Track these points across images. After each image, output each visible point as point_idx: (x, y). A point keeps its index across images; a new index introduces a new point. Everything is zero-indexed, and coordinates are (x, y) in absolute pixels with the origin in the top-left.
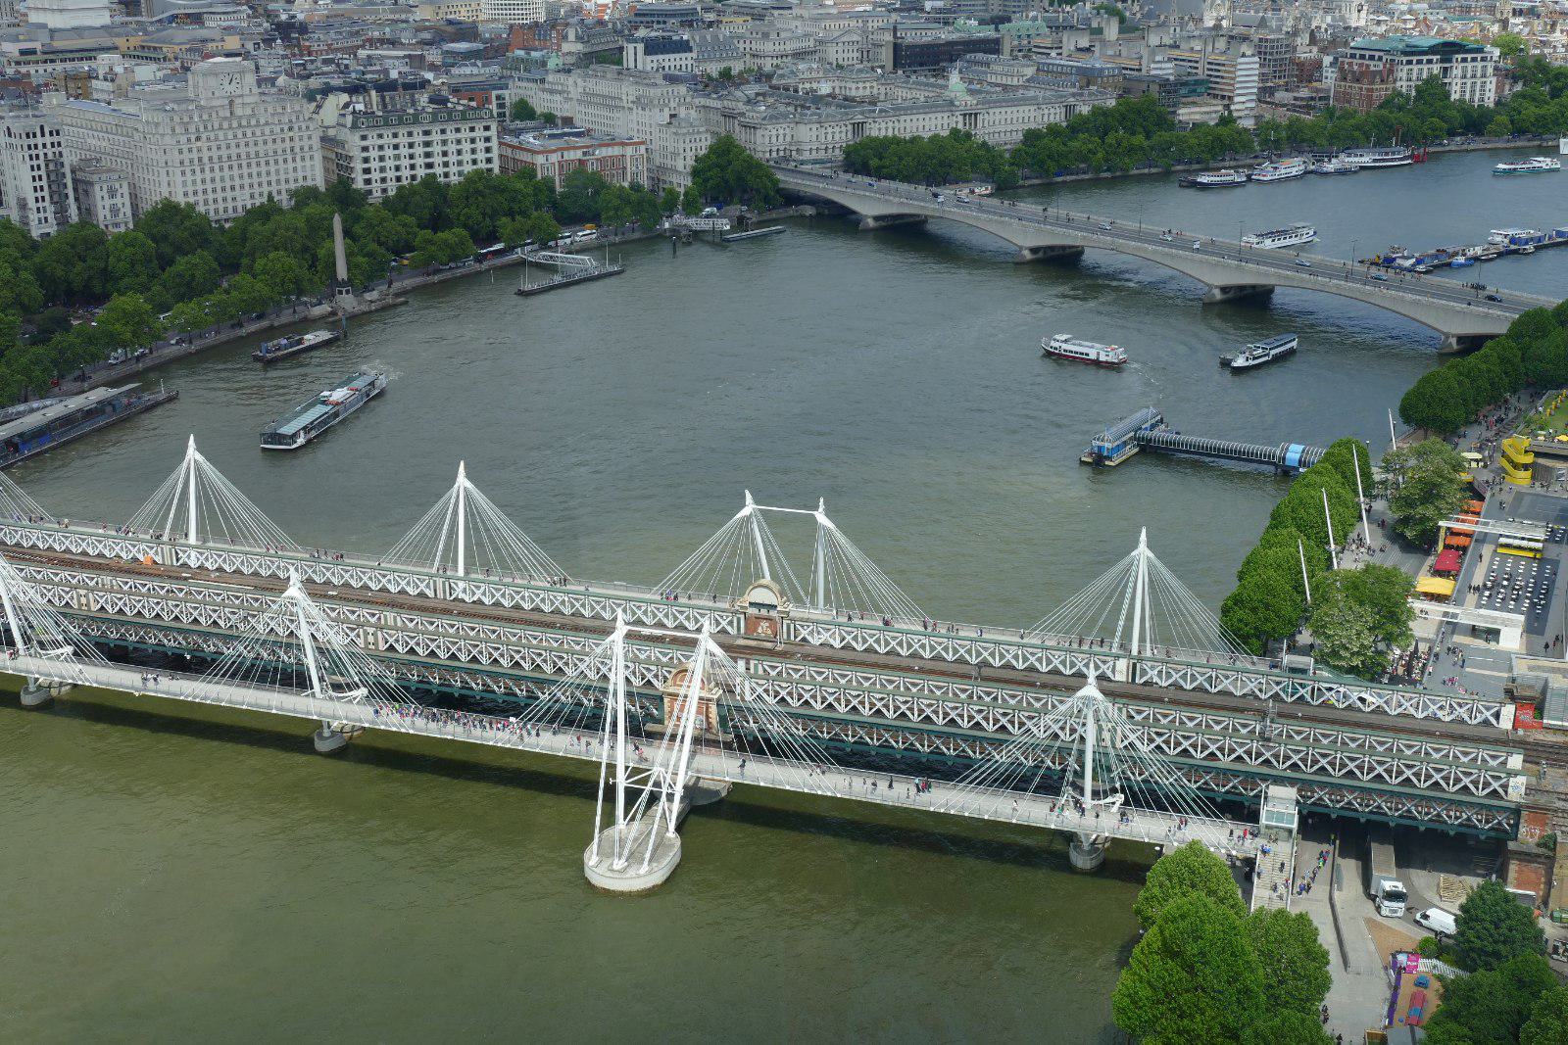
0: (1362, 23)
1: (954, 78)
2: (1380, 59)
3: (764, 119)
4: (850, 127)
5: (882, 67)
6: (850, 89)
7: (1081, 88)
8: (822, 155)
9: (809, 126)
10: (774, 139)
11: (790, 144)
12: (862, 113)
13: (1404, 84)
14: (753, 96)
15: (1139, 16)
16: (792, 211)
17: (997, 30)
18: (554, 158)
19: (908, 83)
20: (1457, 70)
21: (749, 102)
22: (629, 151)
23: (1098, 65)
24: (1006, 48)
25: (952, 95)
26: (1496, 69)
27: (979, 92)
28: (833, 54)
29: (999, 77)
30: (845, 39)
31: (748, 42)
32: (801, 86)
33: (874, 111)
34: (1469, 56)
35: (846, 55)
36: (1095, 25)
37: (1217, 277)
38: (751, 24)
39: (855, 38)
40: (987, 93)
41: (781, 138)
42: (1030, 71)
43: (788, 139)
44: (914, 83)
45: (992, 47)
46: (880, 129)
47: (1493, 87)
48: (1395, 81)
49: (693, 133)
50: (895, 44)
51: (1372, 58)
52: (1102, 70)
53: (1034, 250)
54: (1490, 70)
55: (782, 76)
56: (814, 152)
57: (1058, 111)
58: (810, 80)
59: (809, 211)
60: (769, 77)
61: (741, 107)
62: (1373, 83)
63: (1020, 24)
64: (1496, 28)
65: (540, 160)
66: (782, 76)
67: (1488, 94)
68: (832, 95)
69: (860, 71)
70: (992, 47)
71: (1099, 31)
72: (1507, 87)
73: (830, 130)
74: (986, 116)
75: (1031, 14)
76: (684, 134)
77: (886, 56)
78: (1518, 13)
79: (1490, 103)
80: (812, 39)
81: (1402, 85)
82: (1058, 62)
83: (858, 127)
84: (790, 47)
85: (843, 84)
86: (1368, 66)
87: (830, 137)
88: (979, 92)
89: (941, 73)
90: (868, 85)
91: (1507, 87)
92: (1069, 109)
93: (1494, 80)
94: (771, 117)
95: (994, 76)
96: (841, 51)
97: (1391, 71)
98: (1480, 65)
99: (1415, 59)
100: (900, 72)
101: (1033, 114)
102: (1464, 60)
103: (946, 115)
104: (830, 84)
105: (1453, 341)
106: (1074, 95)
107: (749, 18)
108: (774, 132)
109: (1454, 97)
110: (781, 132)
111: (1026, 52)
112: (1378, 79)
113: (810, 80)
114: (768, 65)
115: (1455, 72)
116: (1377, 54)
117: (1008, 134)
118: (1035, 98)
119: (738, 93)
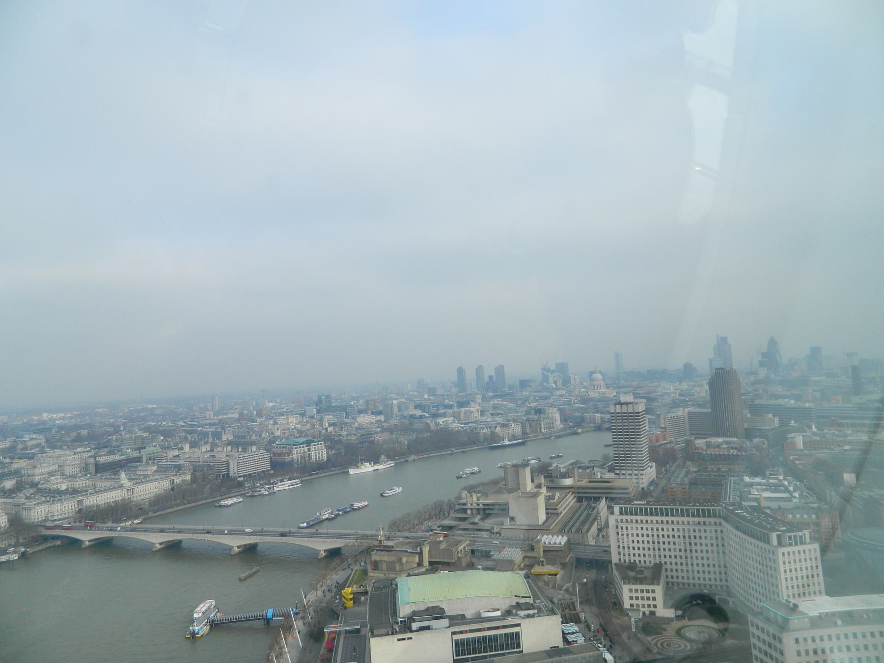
0: (279, 434)
1: (123, 475)
2: (286, 448)
3: (35, 505)
4: (76, 503)
5: (90, 473)
6: (76, 485)
7: (176, 472)
8: (64, 516)
10: (39, 513)
11: (48, 513)
12: (82, 496)
13: (296, 455)
14: (29, 495)
15: (197, 440)
16: (49, 545)
17: (140, 453)
19: (102, 479)
20: (313, 448)
21: (27, 498)
23: (182, 463)
24: (144, 460)
25: (122, 482)
26: (325, 446)
27: (134, 479)
28: (68, 470)
29: (142, 472)
30: (73, 463)
31: (26, 470)
32: (52, 487)
34: (316, 444)
35: (73, 470)
36: (180, 446)
37: (235, 543)
38: (27, 462)
39: (77, 462)
40: (137, 479)
41: (43, 512)
42: (155, 468)
43: (47, 512)
44: (105, 479)
45: (139, 460)
46: (90, 501)
47: (325, 453)
48: (293, 455)
50: (96, 464)
51: (284, 448)
52: (184, 464)
53: (161, 544)
54: (324, 447)
55: (43, 484)
56: (59, 516)
57: (167, 482)
58: (57, 484)
59: (58, 543)
60: (36, 485)
61: (23, 501)
62: (285, 456)
63: (150, 449)
64: (324, 431)
66: (43, 484)
67: (324, 455)
68: (67, 490)
69: (80, 477)
70: (139, 460)
71: (182, 449)
72: (330, 452)
75: (154, 444)
77: (92, 468)
78: (330, 425)
79: (325, 458)
80: (57, 466)
81: (295, 456)
82: (166, 463)
83: (80, 502)
84: (46, 470)
85: (73, 483)
86: (282, 451)
87: (67, 508)
88: (134, 479)
89: (117, 473)
90: (84, 482)
91: (330, 452)
92: (172, 482)
93: (325, 450)
94: (38, 504)
95: (140, 472)
96: (71, 468)
97: (291, 452)
98: (320, 446)
99: (298, 446)
100: (99, 475)
101: (157, 486)
102: (315, 445)
103: (119, 491)
104: (66, 484)
105: (322, 552)
106: (173, 476)
107: (27, 460)
108: (39, 510)
109: (313, 457)
110: (43, 509)
111: (152, 459)
112: (287, 455)
113: (57, 484)
114: (37, 479)
115: (312, 449)
116: (285, 446)
117: (147, 495)
118: (157, 479)
119: (21, 495)
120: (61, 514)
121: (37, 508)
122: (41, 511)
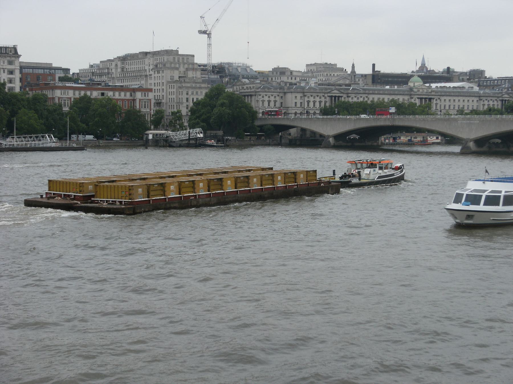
9: (294, 95)
12: (338, 90)
18: (71, 93)
22: (139, 95)
33: (349, 89)
43: (277, 104)
49: (195, 88)
65: (58, 93)
73: (312, 99)
74: (438, 101)
76: (188, 88)
87: (311, 105)
108: (266, 99)
110: (272, 99)
120: (301, 114)
121: (263, 94)
122: (269, 102)
